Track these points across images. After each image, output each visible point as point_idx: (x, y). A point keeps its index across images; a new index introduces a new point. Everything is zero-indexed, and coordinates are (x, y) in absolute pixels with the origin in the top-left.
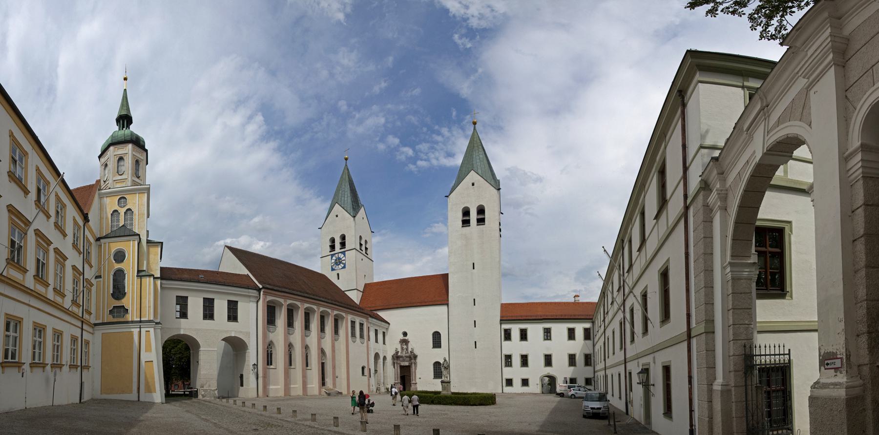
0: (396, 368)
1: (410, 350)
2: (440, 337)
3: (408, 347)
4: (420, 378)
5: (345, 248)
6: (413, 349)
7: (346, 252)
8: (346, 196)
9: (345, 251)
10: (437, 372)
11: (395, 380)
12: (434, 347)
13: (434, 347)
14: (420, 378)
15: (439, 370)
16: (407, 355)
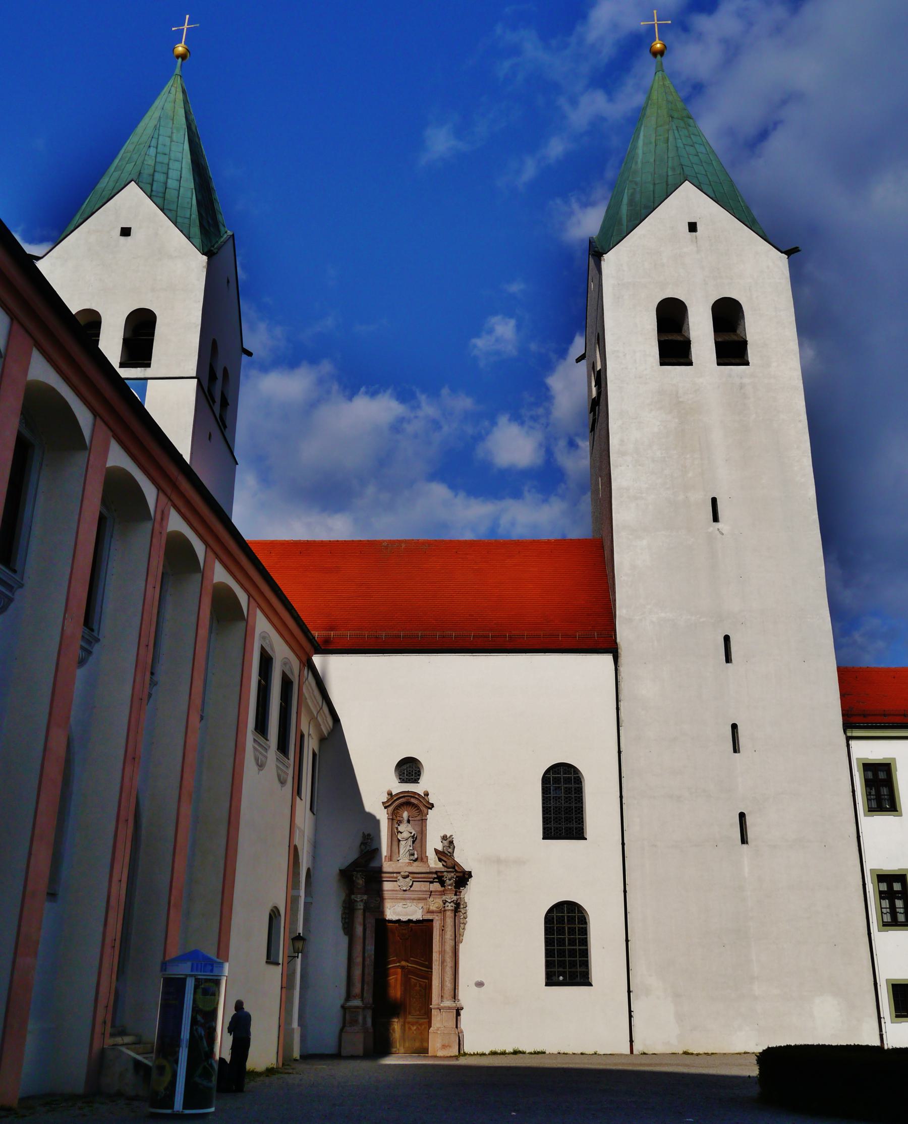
0: (359, 930)
1: (433, 843)
2: (579, 791)
3: (423, 832)
4: (480, 984)
5: (148, 365)
6: (449, 842)
7: (149, 381)
8: (174, 174)
9: (147, 379)
10: (561, 953)
11: (349, 996)
12: (550, 833)
13: (550, 833)
14: (480, 984)
15: (572, 942)
16: (417, 867)
